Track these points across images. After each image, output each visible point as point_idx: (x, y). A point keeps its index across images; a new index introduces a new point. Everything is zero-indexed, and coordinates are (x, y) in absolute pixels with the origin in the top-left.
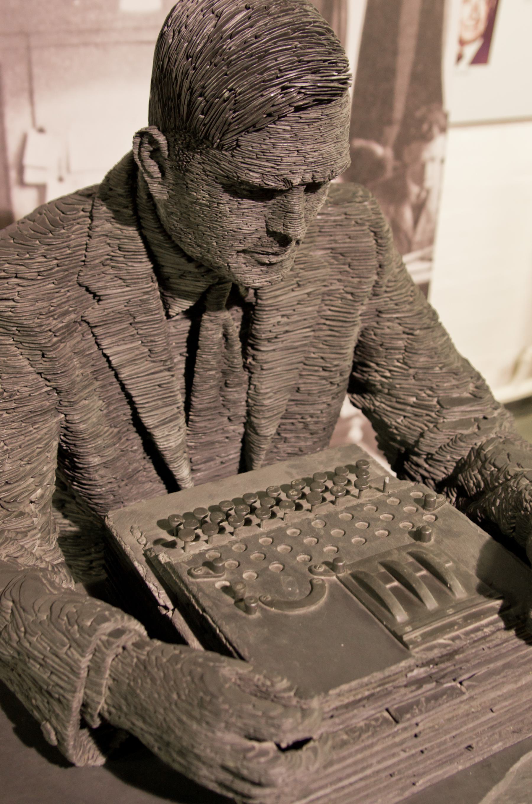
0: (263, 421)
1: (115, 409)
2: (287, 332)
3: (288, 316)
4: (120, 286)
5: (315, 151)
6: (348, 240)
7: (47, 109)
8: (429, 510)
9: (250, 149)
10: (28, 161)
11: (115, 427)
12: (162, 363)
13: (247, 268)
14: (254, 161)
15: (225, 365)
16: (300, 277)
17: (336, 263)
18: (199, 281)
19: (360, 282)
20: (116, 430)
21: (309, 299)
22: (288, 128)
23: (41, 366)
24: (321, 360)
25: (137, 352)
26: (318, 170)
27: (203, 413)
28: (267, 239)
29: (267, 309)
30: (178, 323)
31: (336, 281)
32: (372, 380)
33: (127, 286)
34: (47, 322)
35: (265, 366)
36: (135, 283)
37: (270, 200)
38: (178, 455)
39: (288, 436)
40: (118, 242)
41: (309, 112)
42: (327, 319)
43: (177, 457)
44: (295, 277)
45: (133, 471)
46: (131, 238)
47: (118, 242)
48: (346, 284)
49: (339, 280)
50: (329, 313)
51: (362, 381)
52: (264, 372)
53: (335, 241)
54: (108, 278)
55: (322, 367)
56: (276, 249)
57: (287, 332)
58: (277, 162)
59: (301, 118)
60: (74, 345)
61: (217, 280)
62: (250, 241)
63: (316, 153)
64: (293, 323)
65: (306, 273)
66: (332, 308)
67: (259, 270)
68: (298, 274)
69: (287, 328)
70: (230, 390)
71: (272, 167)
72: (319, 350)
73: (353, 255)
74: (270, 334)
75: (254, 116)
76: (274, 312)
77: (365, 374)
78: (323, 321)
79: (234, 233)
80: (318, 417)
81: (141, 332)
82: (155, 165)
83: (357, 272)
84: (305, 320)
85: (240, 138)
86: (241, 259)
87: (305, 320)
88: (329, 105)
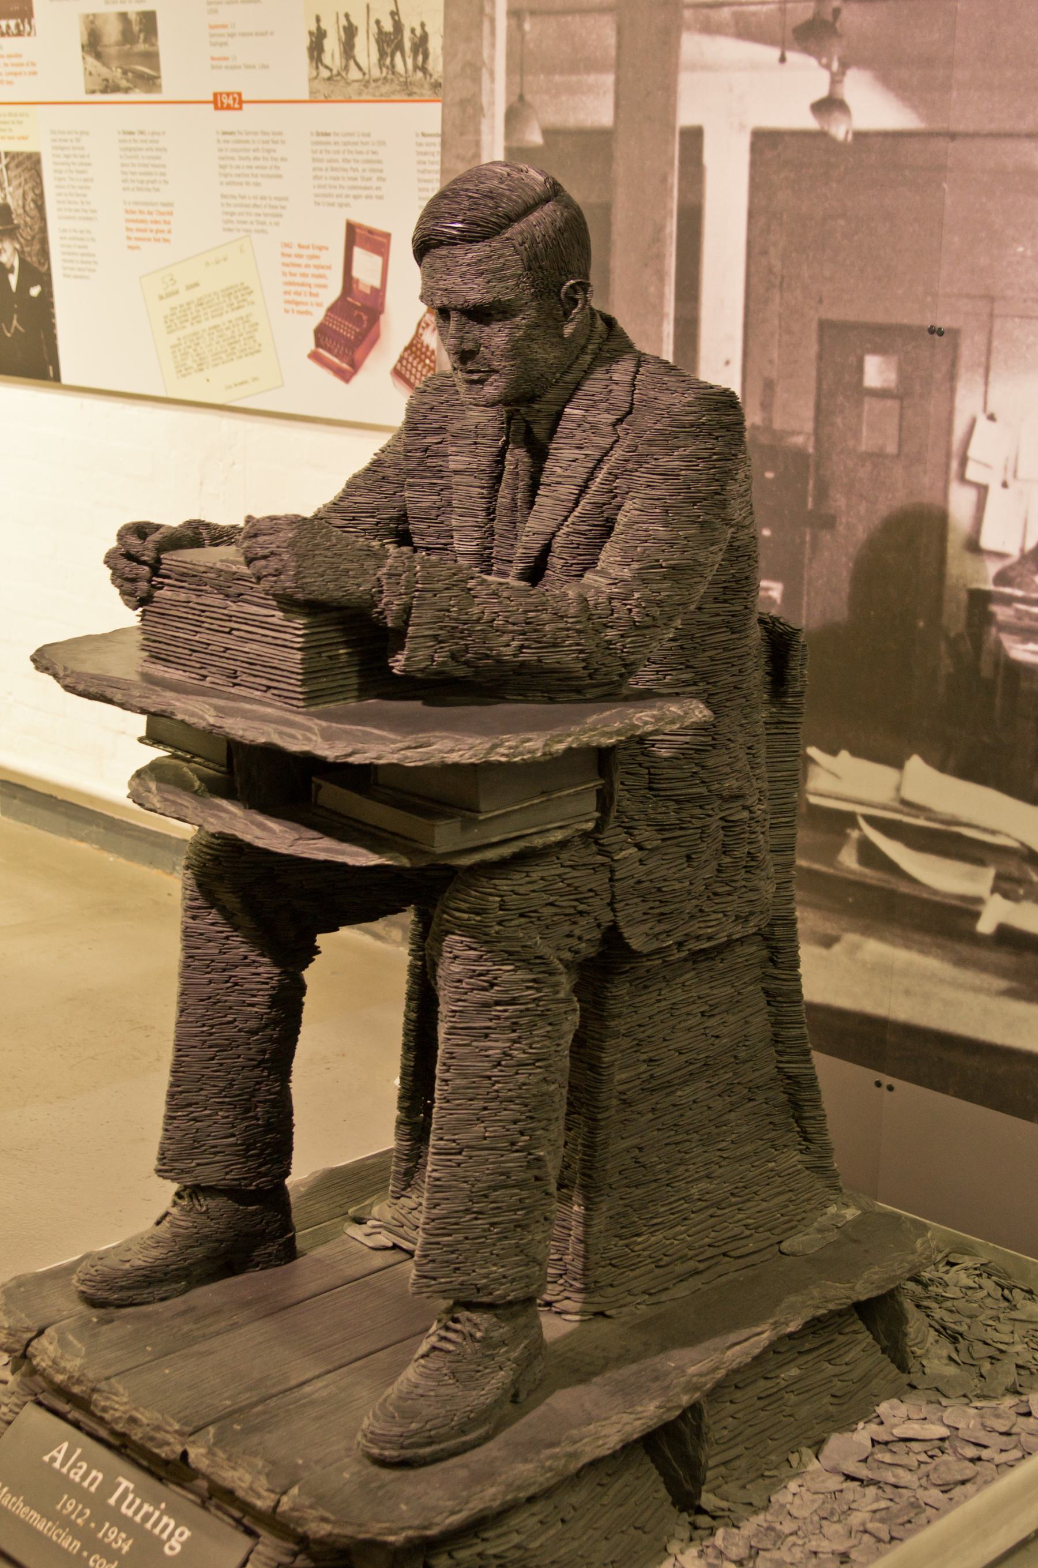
2: (560, 483)
7: (1003, 393)
10: (972, 452)
57: (560, 483)
69: (559, 480)
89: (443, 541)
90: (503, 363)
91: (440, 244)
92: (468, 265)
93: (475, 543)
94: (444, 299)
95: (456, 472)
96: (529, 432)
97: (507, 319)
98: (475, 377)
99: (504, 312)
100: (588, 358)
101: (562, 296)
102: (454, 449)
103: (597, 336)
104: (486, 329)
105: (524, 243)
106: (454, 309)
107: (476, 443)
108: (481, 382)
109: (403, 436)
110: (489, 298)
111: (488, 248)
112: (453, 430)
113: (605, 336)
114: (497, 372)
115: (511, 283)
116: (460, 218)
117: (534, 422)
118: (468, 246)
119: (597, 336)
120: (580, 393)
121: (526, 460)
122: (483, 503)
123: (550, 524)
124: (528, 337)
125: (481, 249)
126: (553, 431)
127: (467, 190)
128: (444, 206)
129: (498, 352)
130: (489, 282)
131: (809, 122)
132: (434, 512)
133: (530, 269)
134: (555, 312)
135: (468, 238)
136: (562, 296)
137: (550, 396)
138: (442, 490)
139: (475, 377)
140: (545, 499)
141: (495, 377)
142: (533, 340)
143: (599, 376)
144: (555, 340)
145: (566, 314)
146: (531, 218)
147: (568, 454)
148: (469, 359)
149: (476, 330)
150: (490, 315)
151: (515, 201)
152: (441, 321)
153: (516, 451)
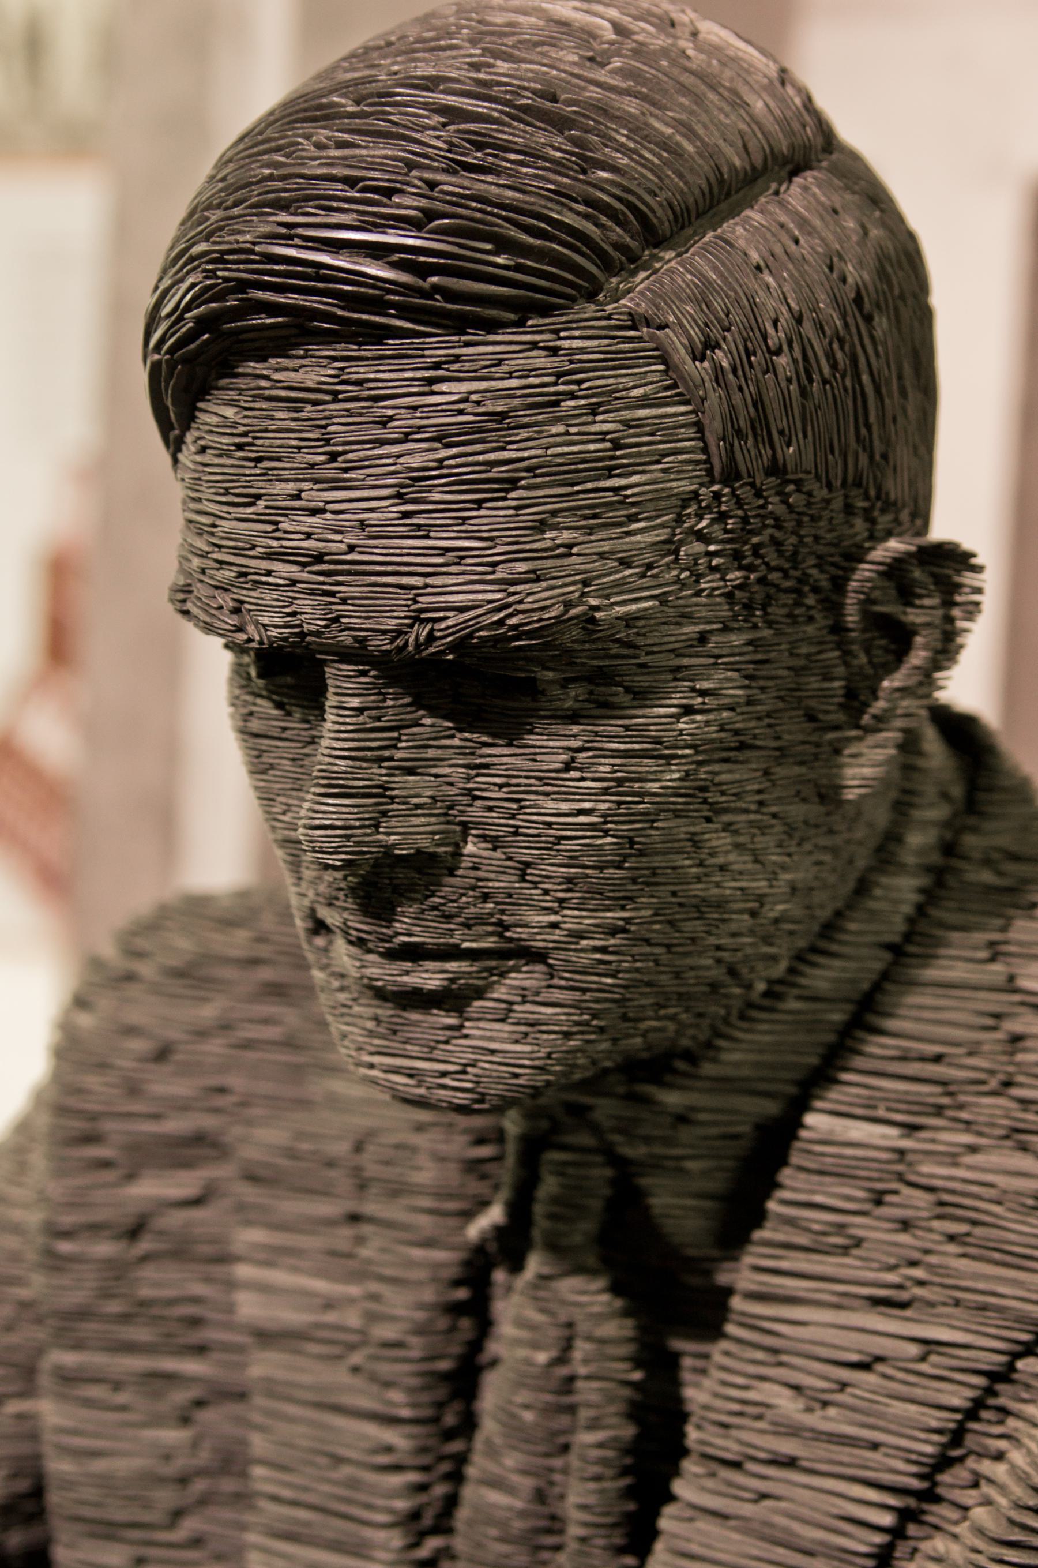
2: (791, 1463)
5: (314, 512)
16: (930, 1267)
25: (331, 1317)
41: (297, 363)
44: (913, 1263)
57: (791, 1463)
61: (544, 1124)
63: (315, 520)
65: (963, 1264)
69: (787, 1447)
76: (760, 1355)
87: (875, 1446)
88: (370, 350)
90: (571, 920)
91: (299, 332)
92: (442, 438)
94: (305, 604)
95: (267, 1337)
96: (626, 1200)
97: (606, 708)
98: (429, 977)
99: (601, 677)
100: (903, 889)
101: (852, 616)
102: (256, 1235)
103: (930, 791)
104: (503, 756)
105: (710, 345)
106: (345, 656)
107: (355, 1218)
108: (452, 999)
109: (39, 1160)
110: (541, 602)
111: (540, 360)
112: (250, 1153)
113: (957, 791)
114: (539, 957)
115: (644, 536)
116: (408, 204)
117: (655, 1165)
118: (438, 347)
119: (930, 791)
120: (877, 1046)
121: (611, 1329)
122: (393, 1492)
124: (700, 798)
125: (506, 364)
126: (740, 1214)
127: (431, 83)
128: (317, 154)
129: (553, 868)
130: (541, 526)
132: (166, 1498)
133: (730, 475)
134: (814, 682)
135: (444, 304)
136: (852, 616)
137: (735, 1058)
138: (200, 1404)
139: (429, 977)
140: (705, 1525)
141: (525, 977)
142: (718, 810)
143: (958, 972)
144: (797, 811)
145: (856, 700)
146: (735, 230)
148: (402, 893)
149: (448, 758)
150: (531, 688)
151: (665, 144)
152: (265, 706)
153: (570, 1287)
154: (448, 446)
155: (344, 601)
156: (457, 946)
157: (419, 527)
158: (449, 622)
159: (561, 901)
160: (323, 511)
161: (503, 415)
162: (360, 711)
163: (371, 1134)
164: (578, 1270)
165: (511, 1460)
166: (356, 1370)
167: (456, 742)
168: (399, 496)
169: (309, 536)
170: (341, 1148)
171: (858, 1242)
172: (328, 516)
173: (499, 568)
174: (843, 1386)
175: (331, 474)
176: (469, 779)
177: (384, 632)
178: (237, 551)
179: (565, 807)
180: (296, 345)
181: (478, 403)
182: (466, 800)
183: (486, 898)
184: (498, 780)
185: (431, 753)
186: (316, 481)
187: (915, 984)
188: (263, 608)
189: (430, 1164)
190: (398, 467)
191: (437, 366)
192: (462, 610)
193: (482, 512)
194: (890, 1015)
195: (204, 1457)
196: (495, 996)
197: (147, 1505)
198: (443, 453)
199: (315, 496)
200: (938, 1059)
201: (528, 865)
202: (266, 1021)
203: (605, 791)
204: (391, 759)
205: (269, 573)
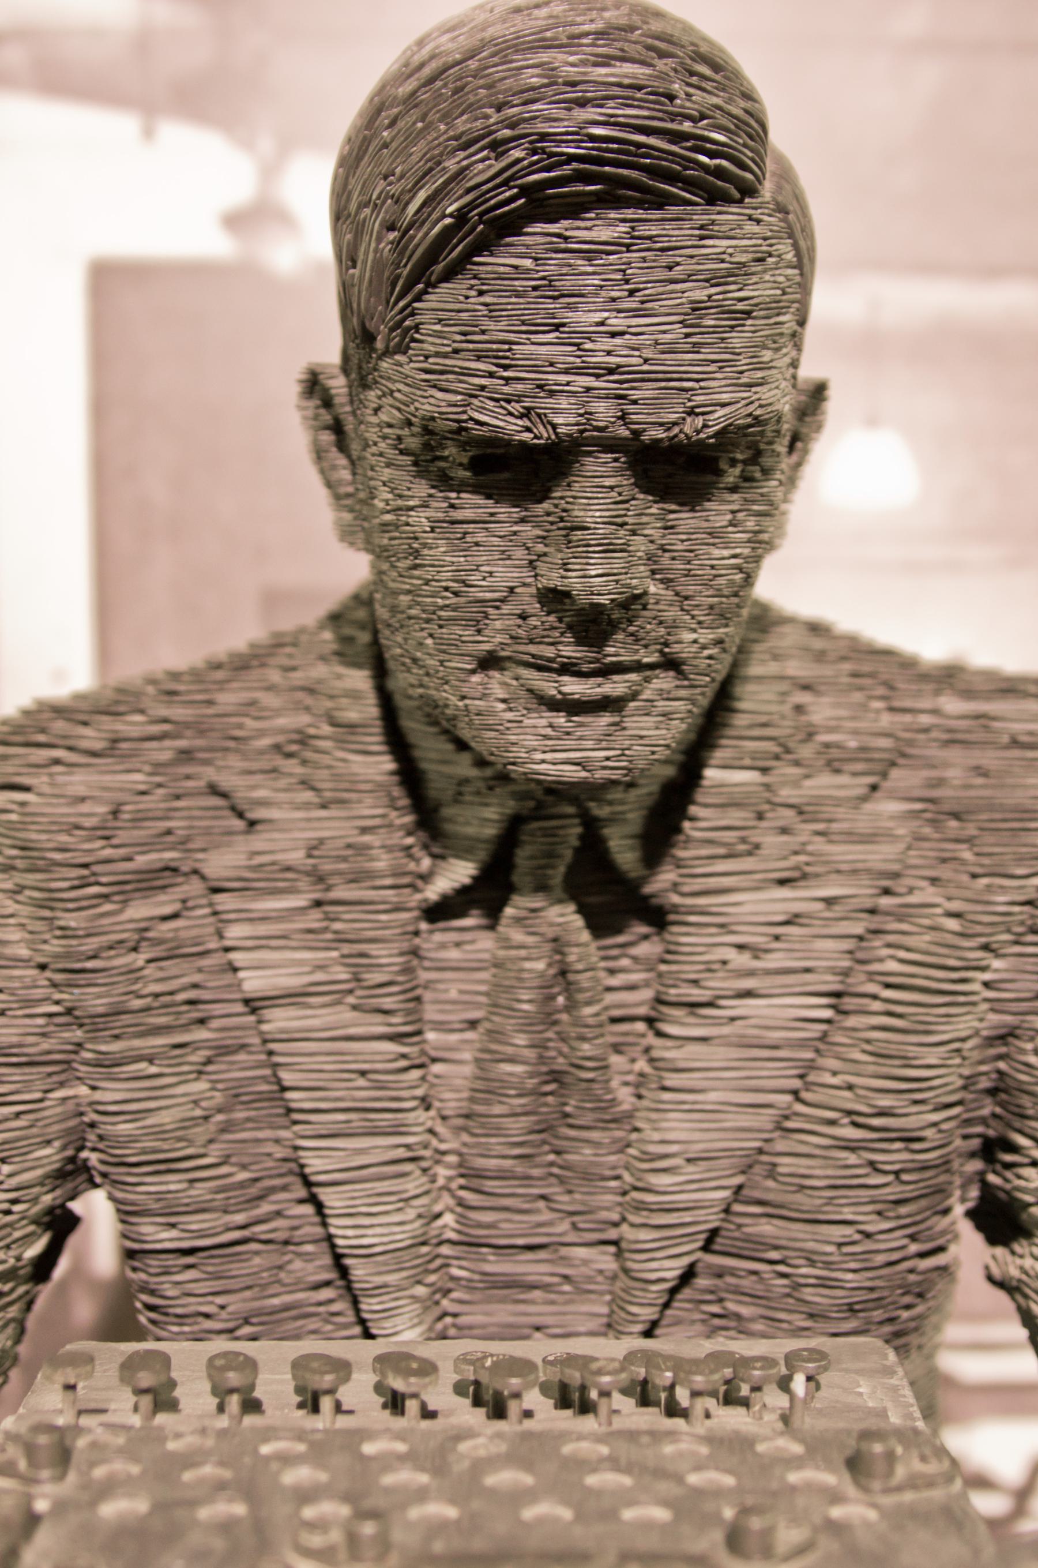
0: (644, 1235)
1: (248, 1120)
2: (748, 994)
3: (756, 952)
4: (307, 806)
5: (613, 335)
6: (980, 781)
8: (866, 1490)
9: (438, 327)
11: (244, 1167)
12: (379, 1018)
13: (510, 715)
14: (448, 362)
15: (561, 1060)
16: (811, 854)
17: (936, 836)
18: (487, 805)
19: (988, 886)
20: (243, 1176)
21: (827, 914)
22: (528, 263)
23: (46, 947)
24: (847, 1094)
25: (320, 976)
26: (635, 394)
27: (490, 1185)
28: (540, 619)
29: (692, 919)
30: (467, 936)
31: (924, 884)
32: (1018, 1189)
33: (324, 806)
34: (87, 846)
35: (672, 1080)
36: (342, 802)
37: (540, 502)
38: (391, 1278)
39: (745, 1311)
40: (329, 704)
41: (589, 224)
42: (888, 986)
43: (385, 1286)
44: (796, 853)
45: (286, 1308)
46: (354, 695)
47: (329, 704)
48: (953, 892)
49: (934, 881)
50: (892, 966)
51: (1002, 1195)
52: (667, 1096)
53: (940, 782)
54: (283, 783)
55: (849, 1113)
56: (570, 651)
57: (748, 994)
58: (502, 360)
59: (566, 239)
60: (152, 919)
61: (532, 804)
62: (498, 624)
63: (618, 341)
64: (768, 972)
66: (902, 954)
67: (544, 722)
68: (804, 844)
70: (572, 1133)
71: (491, 375)
72: (849, 1067)
73: (984, 816)
74: (695, 991)
75: (425, 229)
76: (713, 930)
77: (1008, 1174)
78: (872, 988)
79: (454, 600)
80: (828, 1265)
81: (337, 926)
82: (345, 468)
83: (986, 861)
84: (807, 970)
85: (416, 305)
86: (497, 683)
87: (807, 970)
88: (656, 214)
89: (240, 1218)
90: (705, 636)
93: (411, 1214)
104: (686, 519)
117: (612, 820)
123: (746, 1120)
131: (214, 244)
132: (201, 1133)
138: (209, 1061)
141: (664, 681)
147: (759, 905)
148: (614, 626)
154: (712, 286)
155: (635, 402)
156: (639, 662)
157: (695, 344)
158: (716, 415)
159: (700, 623)
160: (622, 334)
161: (743, 265)
162: (612, 488)
163: (321, 841)
164: (560, 901)
165: (521, 1040)
166: (355, 1008)
167: (653, 511)
168: (680, 322)
169: (609, 353)
170: (297, 857)
171: (757, 846)
172: (627, 337)
173: (746, 374)
174: (777, 938)
175: (634, 305)
176: (664, 536)
177: (661, 424)
178: (535, 369)
179: (726, 553)
180: (588, 210)
181: (731, 255)
182: (660, 553)
183: (661, 623)
184: (684, 537)
185: (645, 519)
186: (619, 311)
187: (746, 679)
188: (557, 411)
189: (384, 856)
190: (684, 300)
191: (702, 228)
192: (723, 405)
193: (734, 334)
194: (739, 699)
195: (219, 1098)
196: (643, 697)
197: (191, 1142)
198: (713, 290)
199: (617, 322)
200: (764, 725)
201: (686, 598)
202: (188, 777)
203: (749, 541)
204: (626, 524)
205: (568, 384)
